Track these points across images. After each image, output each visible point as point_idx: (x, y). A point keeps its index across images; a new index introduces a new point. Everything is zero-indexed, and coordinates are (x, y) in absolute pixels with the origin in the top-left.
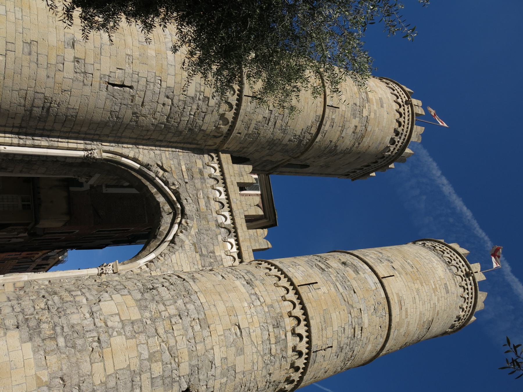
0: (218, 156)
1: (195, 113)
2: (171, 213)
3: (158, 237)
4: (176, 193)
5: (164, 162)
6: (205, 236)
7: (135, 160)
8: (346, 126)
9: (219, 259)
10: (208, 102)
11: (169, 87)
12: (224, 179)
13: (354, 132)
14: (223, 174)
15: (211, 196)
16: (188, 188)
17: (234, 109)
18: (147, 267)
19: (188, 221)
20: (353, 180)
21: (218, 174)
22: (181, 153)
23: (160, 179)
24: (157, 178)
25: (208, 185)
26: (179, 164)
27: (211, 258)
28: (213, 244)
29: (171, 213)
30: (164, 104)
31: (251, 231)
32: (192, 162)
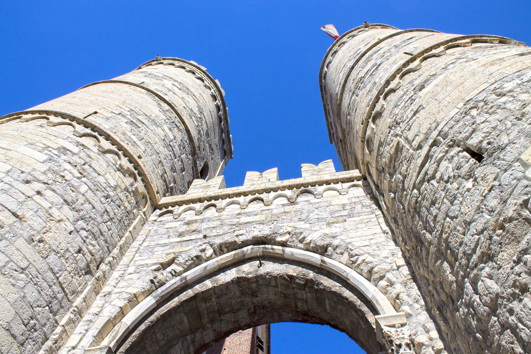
0: (166, 205)
1: (81, 173)
2: (261, 264)
3: (309, 278)
4: (221, 249)
5: (155, 261)
6: (311, 215)
7: (134, 300)
8: (171, 88)
9: (354, 200)
10: (71, 151)
11: (9, 171)
12: (210, 199)
13: (180, 89)
14: (200, 200)
15: (238, 211)
16: (216, 234)
17: (98, 136)
18: (382, 278)
19: (281, 231)
20: (231, 158)
21: (198, 206)
22: (146, 244)
23: (186, 270)
24: (184, 275)
25: (217, 214)
26: (165, 245)
27: (354, 208)
28: (328, 206)
29: (261, 264)
30: (39, 193)
31: (303, 175)
32: (168, 232)
